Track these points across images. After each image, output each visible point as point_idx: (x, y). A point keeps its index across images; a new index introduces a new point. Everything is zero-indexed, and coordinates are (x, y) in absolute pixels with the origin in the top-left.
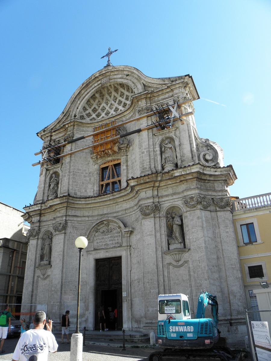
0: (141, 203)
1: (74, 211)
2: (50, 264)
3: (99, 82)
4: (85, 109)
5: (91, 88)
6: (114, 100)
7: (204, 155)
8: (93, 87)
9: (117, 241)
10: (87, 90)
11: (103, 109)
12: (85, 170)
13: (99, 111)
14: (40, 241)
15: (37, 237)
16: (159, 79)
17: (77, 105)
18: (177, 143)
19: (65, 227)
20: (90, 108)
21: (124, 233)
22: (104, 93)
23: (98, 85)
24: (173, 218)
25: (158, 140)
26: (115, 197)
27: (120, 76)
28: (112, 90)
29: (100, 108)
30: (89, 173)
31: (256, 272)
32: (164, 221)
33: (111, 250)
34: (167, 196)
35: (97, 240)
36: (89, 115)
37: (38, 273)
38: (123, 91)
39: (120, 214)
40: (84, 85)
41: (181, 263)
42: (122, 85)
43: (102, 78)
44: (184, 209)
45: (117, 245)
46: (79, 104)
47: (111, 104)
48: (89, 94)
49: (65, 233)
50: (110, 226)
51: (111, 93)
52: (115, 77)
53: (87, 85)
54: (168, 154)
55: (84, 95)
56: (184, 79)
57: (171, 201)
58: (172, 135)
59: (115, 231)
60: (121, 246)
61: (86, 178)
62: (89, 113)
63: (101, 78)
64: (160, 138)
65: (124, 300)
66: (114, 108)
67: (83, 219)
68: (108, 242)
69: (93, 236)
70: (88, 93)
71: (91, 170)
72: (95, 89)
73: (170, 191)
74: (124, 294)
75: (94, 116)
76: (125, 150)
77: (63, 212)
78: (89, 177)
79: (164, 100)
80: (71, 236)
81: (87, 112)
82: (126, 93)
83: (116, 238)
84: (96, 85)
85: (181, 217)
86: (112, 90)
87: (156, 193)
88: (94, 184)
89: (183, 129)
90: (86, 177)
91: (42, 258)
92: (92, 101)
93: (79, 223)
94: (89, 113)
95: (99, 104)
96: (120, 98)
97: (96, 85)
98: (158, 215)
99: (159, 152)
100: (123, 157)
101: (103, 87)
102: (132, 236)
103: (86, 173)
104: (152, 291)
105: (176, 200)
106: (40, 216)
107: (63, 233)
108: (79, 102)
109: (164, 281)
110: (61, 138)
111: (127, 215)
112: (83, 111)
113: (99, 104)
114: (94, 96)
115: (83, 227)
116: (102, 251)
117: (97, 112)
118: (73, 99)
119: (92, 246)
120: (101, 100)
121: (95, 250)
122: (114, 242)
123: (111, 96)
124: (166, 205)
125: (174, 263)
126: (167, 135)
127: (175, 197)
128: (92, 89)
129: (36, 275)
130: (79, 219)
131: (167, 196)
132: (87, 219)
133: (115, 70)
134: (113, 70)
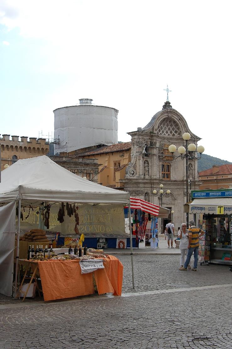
11: (162, 128)
13: (160, 128)
28: (169, 120)
38: (173, 124)
42: (175, 122)
43: (169, 113)
58: (192, 163)
82: (174, 126)
86: (169, 120)
96: (170, 127)
123: (166, 123)
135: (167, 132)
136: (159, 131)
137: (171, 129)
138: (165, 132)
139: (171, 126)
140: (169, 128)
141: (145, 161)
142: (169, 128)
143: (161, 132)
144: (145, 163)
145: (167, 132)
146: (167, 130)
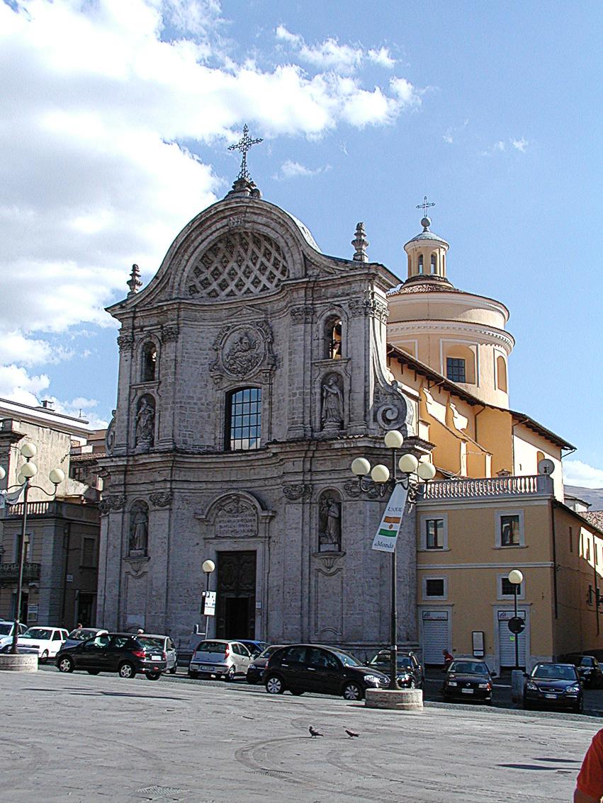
0: (285, 479)
1: (183, 473)
2: (146, 555)
3: (225, 221)
4: (198, 271)
5: (210, 232)
6: (252, 260)
7: (385, 411)
8: (213, 228)
9: (250, 528)
10: (201, 234)
11: (232, 274)
12: (200, 399)
13: (225, 276)
14: (127, 516)
15: (121, 510)
16: (329, 257)
17: (184, 262)
18: (347, 388)
19: (169, 501)
20: (207, 269)
21: (261, 518)
22: (233, 242)
23: (223, 227)
24: (330, 506)
25: (319, 375)
26: (249, 458)
27: (264, 220)
29: (227, 270)
30: (208, 404)
31: (436, 588)
32: (316, 508)
33: (242, 540)
34: (323, 472)
35: (220, 522)
36: (205, 283)
37: (128, 567)
38: (269, 247)
39: (256, 484)
40: (196, 224)
41: (333, 570)
44: (344, 496)
45: (250, 534)
46: (188, 261)
47: (247, 267)
48: (205, 243)
49: (170, 510)
50: (240, 503)
51: (247, 244)
52: (255, 218)
53: (201, 224)
54: (331, 403)
55: (196, 244)
56: (369, 268)
57: (329, 481)
59: (247, 513)
60: (255, 536)
61: (203, 413)
62: (206, 279)
63: (229, 214)
64: (324, 371)
65: (257, 613)
66: (252, 276)
67: (198, 485)
68: (238, 529)
69: (214, 515)
70: (203, 241)
71: (210, 399)
72: (216, 235)
73: (328, 466)
74: (258, 605)
75: (214, 286)
76: (268, 374)
77: (166, 474)
78: (207, 412)
79: (336, 299)
80: (180, 515)
81: (202, 277)
82: (275, 254)
83: (249, 524)
84: (219, 225)
85: (339, 505)
86: (249, 240)
87: (308, 466)
88: (215, 425)
89: (358, 364)
90: (202, 411)
91: (132, 544)
92: (211, 256)
93: (193, 493)
94: (206, 279)
95: (225, 262)
96: (264, 260)
97: (219, 225)
98: (308, 501)
99: (318, 397)
100: (265, 386)
101: (232, 233)
102: (273, 523)
103: (202, 404)
104: (293, 604)
105: (335, 481)
106: (125, 475)
107: (166, 509)
108: (186, 257)
109: (309, 592)
110: (154, 327)
111: (266, 488)
112: (194, 275)
113: (225, 263)
114: (215, 247)
115: (199, 500)
116: (229, 541)
117: (222, 277)
118: (176, 249)
119: (213, 532)
120: (228, 255)
121: (217, 537)
122: (246, 529)
124: (321, 487)
125: (325, 570)
126: (333, 369)
127: (333, 476)
128: (211, 234)
129: (124, 571)
130: (192, 486)
131: (323, 472)
132: (204, 486)
133: (255, 205)
134: (251, 205)
135: (256, 282)
136: (223, 286)
137: (269, 265)
138: (248, 284)
139: (267, 254)
140: (262, 264)
141: (141, 397)
142: (262, 264)
143: (232, 287)
144: (139, 405)
145: (256, 282)
146: (256, 272)
